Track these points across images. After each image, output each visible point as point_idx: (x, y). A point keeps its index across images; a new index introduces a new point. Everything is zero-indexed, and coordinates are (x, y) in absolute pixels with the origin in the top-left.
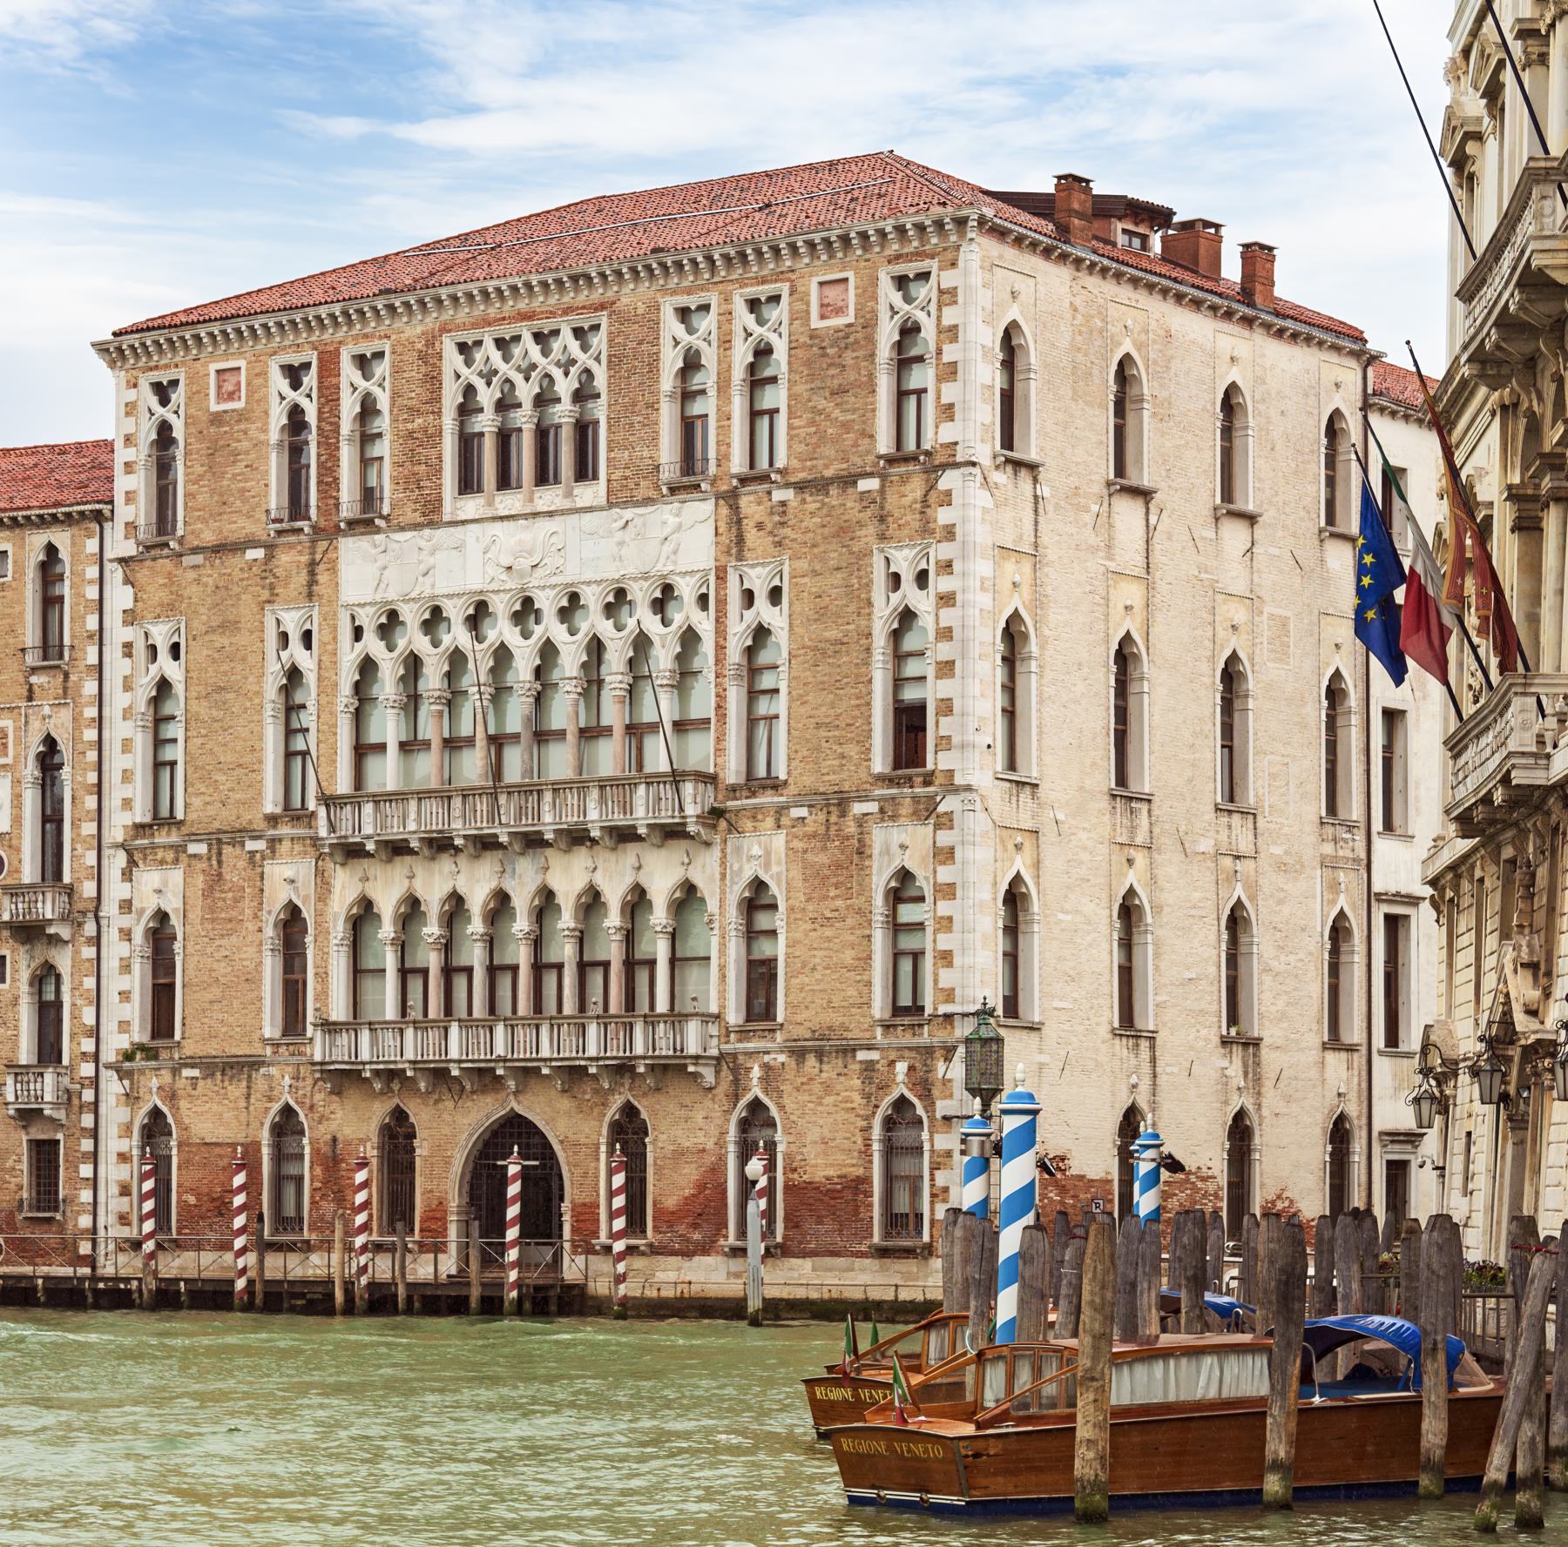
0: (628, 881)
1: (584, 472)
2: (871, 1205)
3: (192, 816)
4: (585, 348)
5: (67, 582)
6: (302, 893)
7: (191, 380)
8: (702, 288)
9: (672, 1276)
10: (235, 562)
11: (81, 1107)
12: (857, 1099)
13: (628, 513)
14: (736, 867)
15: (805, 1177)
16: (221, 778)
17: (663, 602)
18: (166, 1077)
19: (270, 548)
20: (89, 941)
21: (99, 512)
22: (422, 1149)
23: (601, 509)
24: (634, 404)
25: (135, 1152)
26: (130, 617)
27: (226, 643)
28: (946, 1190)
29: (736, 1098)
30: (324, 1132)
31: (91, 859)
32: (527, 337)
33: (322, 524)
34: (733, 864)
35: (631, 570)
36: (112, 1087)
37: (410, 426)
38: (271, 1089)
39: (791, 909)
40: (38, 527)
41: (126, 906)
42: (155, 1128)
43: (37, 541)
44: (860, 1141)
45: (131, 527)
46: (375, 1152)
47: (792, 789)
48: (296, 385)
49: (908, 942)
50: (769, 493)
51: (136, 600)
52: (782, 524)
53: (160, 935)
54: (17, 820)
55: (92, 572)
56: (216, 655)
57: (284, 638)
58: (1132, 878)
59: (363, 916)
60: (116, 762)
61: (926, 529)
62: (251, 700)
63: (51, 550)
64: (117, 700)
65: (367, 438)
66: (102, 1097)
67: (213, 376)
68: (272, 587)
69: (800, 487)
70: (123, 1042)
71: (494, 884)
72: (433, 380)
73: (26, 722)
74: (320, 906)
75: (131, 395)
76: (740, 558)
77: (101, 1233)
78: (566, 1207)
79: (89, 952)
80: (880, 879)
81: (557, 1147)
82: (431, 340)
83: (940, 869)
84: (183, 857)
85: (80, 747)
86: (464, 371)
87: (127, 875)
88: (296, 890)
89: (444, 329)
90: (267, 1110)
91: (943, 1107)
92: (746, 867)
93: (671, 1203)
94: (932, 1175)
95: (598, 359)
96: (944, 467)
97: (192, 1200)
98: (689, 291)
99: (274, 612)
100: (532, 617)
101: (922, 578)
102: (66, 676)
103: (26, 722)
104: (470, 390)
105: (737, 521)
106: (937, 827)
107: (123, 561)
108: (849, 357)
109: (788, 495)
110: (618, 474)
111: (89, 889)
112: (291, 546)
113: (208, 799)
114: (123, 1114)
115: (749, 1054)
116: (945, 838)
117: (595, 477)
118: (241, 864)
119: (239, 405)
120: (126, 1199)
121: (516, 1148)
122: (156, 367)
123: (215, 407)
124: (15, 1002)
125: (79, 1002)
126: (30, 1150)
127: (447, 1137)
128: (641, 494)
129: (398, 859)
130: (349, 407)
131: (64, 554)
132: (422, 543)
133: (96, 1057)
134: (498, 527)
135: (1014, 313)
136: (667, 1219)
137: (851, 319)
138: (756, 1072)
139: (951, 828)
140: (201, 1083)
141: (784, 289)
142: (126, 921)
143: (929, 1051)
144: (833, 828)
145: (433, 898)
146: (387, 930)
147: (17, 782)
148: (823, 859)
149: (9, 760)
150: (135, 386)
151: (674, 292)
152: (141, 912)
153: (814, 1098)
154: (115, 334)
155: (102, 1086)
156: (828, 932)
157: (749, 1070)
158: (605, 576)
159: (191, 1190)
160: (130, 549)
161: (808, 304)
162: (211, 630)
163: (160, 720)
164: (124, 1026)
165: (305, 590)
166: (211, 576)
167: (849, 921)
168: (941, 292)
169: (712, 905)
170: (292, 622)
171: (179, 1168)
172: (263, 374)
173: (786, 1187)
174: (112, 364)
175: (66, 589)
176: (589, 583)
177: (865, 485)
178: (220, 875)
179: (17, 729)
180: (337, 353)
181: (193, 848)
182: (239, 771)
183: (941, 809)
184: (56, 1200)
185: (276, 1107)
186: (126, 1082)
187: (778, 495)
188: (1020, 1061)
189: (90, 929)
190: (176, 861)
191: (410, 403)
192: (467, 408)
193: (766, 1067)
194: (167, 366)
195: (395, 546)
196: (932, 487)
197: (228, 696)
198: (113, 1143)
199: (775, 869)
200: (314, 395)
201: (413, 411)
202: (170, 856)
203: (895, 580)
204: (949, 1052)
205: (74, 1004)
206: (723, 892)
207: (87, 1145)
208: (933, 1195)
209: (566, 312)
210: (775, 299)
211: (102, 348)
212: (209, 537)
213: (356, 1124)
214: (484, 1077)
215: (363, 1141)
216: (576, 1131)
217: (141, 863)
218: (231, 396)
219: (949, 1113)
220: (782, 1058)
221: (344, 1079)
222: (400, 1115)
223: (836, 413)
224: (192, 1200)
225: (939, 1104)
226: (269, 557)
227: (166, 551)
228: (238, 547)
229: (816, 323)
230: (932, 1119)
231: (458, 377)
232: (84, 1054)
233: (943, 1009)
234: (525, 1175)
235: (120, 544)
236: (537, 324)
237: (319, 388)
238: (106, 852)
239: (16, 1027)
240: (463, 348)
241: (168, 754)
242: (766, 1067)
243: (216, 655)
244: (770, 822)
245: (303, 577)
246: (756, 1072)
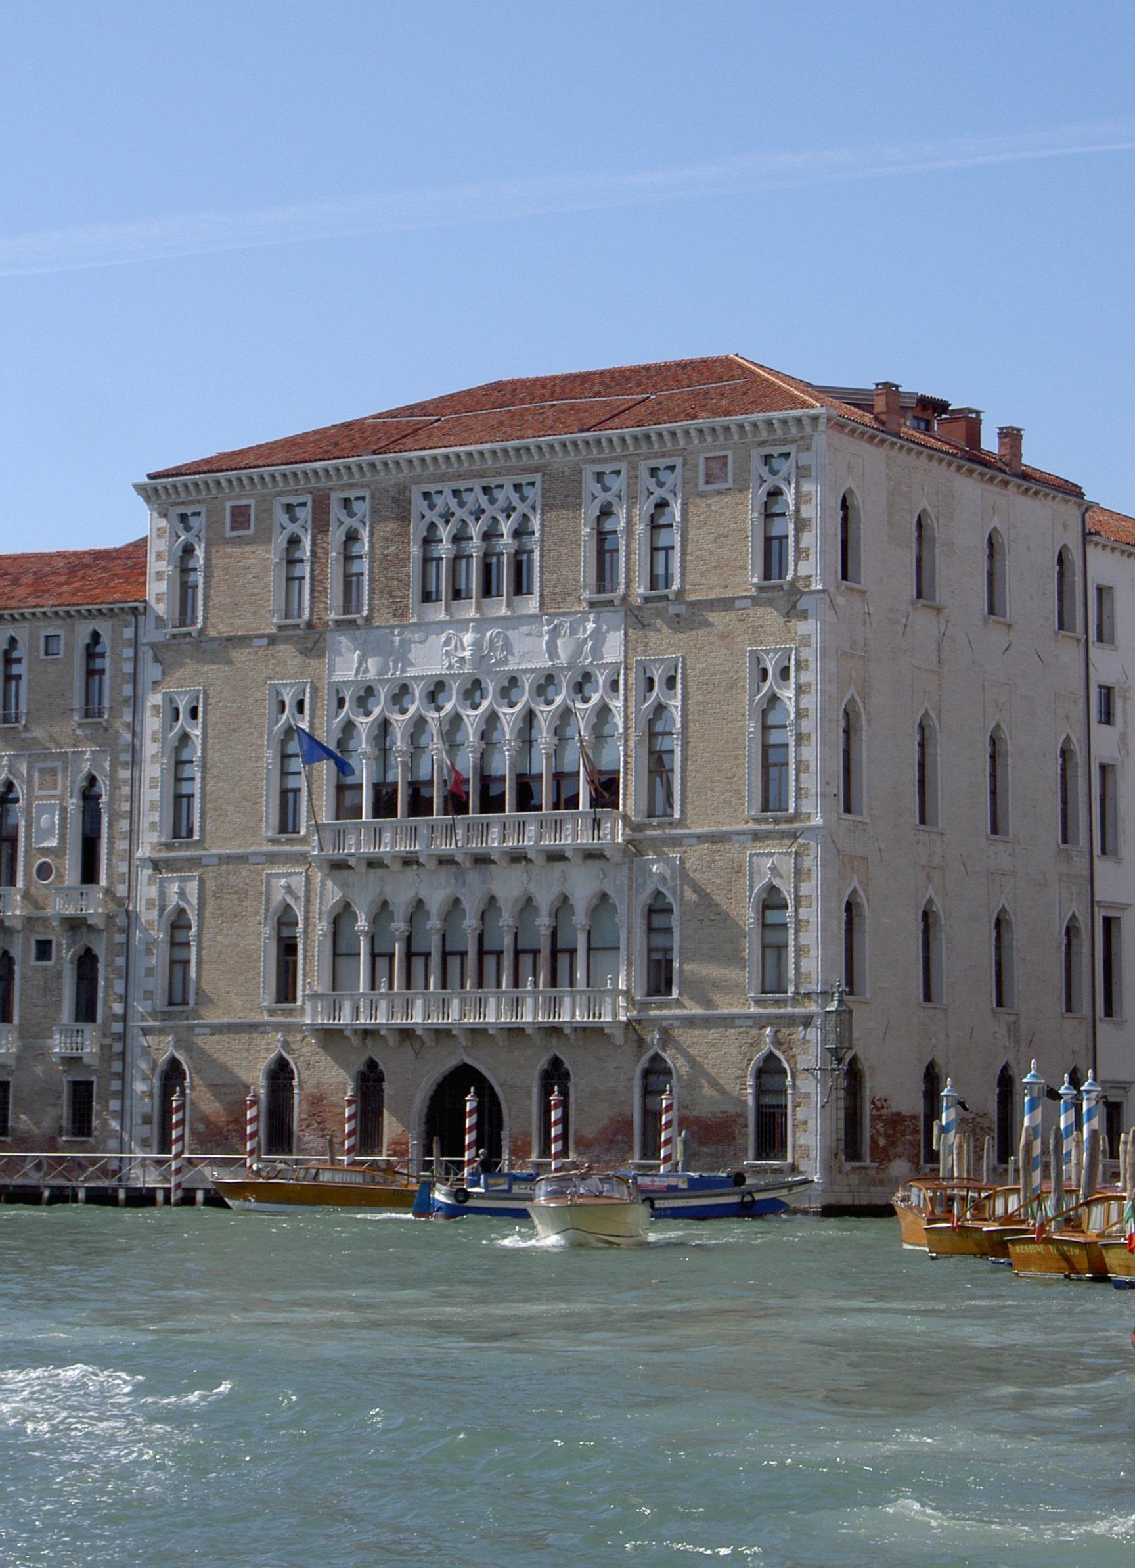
0: (555, 891)
1: (520, 587)
2: (747, 1134)
4: (523, 499)
5: (107, 661)
8: (616, 459)
14: (640, 880)
17: (581, 687)
20: (121, 930)
21: (136, 608)
31: (123, 868)
32: (478, 490)
39: (683, 913)
40: (85, 618)
48: (293, 519)
49: (773, 937)
53: (178, 923)
55: (129, 652)
58: (931, 892)
59: (341, 918)
63: (96, 636)
64: (150, 748)
65: (348, 558)
66: (129, 1047)
71: (448, 891)
78: (505, 1134)
79: (120, 938)
81: (497, 1089)
82: (403, 490)
86: (427, 512)
92: (648, 882)
94: (794, 1111)
95: (534, 508)
97: (201, 1128)
100: (478, 693)
101: (784, 673)
104: (432, 526)
107: (153, 646)
117: (530, 592)
120: (147, 1127)
121: (472, 1089)
122: (183, 503)
123: (229, 534)
124: (59, 975)
125: (111, 976)
129: (372, 871)
130: (336, 536)
131: (106, 639)
133: (124, 1018)
135: (850, 483)
141: (678, 461)
145: (401, 901)
146: (362, 924)
149: (58, 792)
151: (593, 461)
154: (150, 477)
155: (129, 1040)
160: (157, 636)
163: (179, 763)
164: (148, 995)
169: (622, 909)
172: (269, 511)
174: (148, 499)
175: (107, 664)
180: (328, 497)
182: (245, 803)
188: (864, 1026)
192: (429, 541)
194: (191, 503)
196: (794, 606)
200: (309, 526)
206: (630, 899)
207: (116, 1085)
209: (509, 471)
210: (672, 468)
211: (141, 489)
214: (442, 1034)
221: (329, 1037)
222: (372, 1065)
224: (201, 1128)
227: (188, 640)
231: (423, 517)
234: (479, 1110)
235: (151, 634)
236: (485, 482)
239: (60, 995)
240: (426, 495)
241: (185, 788)
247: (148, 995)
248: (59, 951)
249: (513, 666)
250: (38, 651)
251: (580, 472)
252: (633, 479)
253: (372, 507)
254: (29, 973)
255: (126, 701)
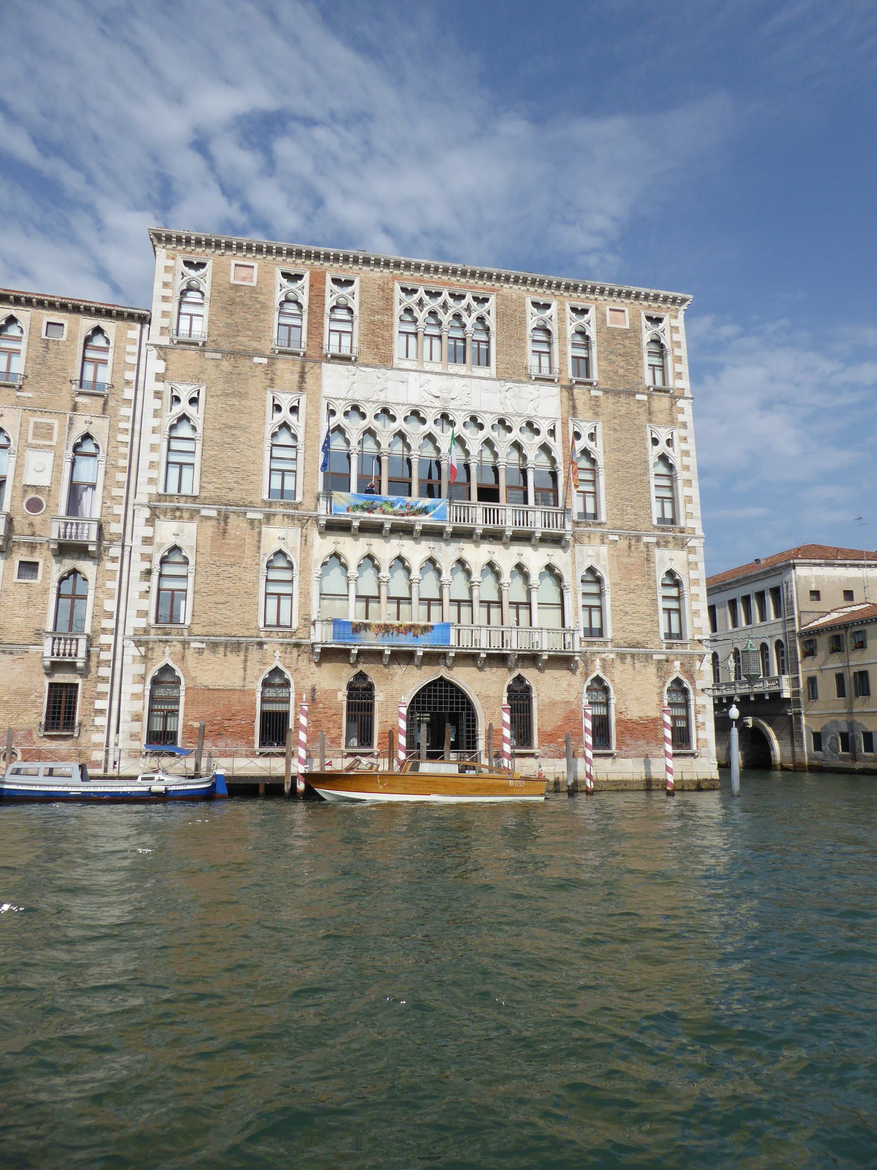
3: (204, 494)
6: (290, 546)
7: (216, 265)
9: (552, 769)
10: (244, 365)
11: (98, 662)
12: (654, 679)
13: (509, 385)
15: (628, 717)
16: (228, 474)
18: (179, 647)
19: (272, 359)
20: (113, 560)
22: (379, 697)
23: (493, 380)
24: (512, 337)
25: (147, 693)
26: (160, 378)
27: (236, 403)
28: (704, 724)
29: (587, 675)
30: (308, 684)
31: (119, 510)
33: (309, 353)
34: (579, 559)
35: (511, 411)
36: (132, 651)
37: (372, 318)
38: (264, 657)
41: (147, 541)
42: (164, 678)
43: (88, 323)
44: (656, 699)
45: (164, 330)
46: (345, 698)
47: (609, 526)
50: (589, 391)
51: (167, 369)
52: (598, 406)
54: (56, 479)
56: (228, 409)
57: (278, 408)
60: (147, 457)
61: (672, 422)
62: (254, 435)
64: (150, 422)
67: (233, 266)
68: (272, 380)
69: (606, 392)
70: (142, 623)
72: (388, 300)
73: (71, 423)
74: (304, 554)
75: (171, 263)
76: (574, 415)
77: (112, 745)
80: (660, 575)
83: (691, 572)
84: (197, 518)
85: (114, 444)
87: (150, 522)
88: (286, 544)
89: (394, 278)
90: (261, 671)
91: (699, 685)
93: (548, 728)
95: (489, 313)
96: (680, 397)
98: (540, 295)
99: (272, 392)
101: (669, 442)
102: (105, 403)
103: (71, 423)
105: (572, 398)
106: (689, 552)
107: (160, 347)
108: (627, 342)
109: (600, 393)
110: (502, 366)
111: (115, 528)
112: (287, 361)
113: (219, 486)
114: (140, 669)
115: (593, 654)
116: (692, 558)
118: (245, 525)
119: (254, 284)
123: (233, 281)
124: (46, 591)
125: (101, 596)
126: (50, 691)
127: (396, 693)
128: (516, 378)
130: (329, 302)
132: (380, 375)
134: (429, 376)
136: (548, 737)
137: (627, 326)
138: (598, 662)
139: (695, 554)
140: (206, 652)
142: (148, 550)
143: (691, 656)
144: (633, 548)
147: (58, 458)
148: (626, 560)
149: (53, 443)
150: (173, 259)
152: (161, 545)
153: (631, 677)
156: (632, 595)
157: (593, 661)
158: (496, 411)
159: (196, 719)
160: (165, 341)
161: (605, 316)
162: (227, 395)
165: (296, 384)
166: (226, 366)
167: (644, 591)
168: (672, 327)
170: (286, 401)
171: (186, 704)
172: (272, 273)
173: (619, 722)
176: (486, 412)
177: (638, 397)
178: (225, 532)
179: (61, 426)
181: (204, 512)
183: (689, 544)
184: (73, 724)
185: (270, 668)
186: (142, 649)
187: (594, 393)
189: (115, 551)
190: (191, 518)
191: (372, 307)
193: (604, 660)
195: (359, 372)
197: (236, 432)
198: (130, 688)
199: (602, 563)
201: (375, 312)
202: (186, 515)
203: (655, 442)
204: (701, 657)
205: (96, 597)
208: (697, 727)
209: (470, 287)
212: (225, 345)
213: (334, 682)
215: (335, 692)
216: (487, 690)
217: (162, 517)
218: (244, 279)
219: (704, 687)
220: (612, 656)
223: (622, 364)
224: (196, 725)
225: (697, 682)
226: (270, 365)
228: (248, 355)
229: (609, 325)
230: (694, 689)
232: (104, 629)
233: (697, 637)
237: (311, 286)
238: (130, 508)
239: (44, 609)
242: (604, 660)
243: (228, 409)
244: (597, 540)
245: (296, 377)
246: (598, 662)
247: (143, 614)
248: (47, 572)
249: (475, 406)
250: (40, 332)
251: (524, 298)
252: (562, 310)
253: (361, 287)
254: (12, 588)
255: (128, 382)
